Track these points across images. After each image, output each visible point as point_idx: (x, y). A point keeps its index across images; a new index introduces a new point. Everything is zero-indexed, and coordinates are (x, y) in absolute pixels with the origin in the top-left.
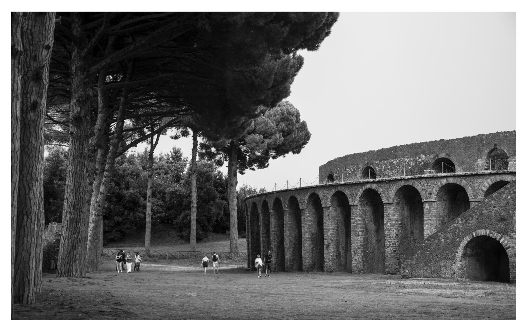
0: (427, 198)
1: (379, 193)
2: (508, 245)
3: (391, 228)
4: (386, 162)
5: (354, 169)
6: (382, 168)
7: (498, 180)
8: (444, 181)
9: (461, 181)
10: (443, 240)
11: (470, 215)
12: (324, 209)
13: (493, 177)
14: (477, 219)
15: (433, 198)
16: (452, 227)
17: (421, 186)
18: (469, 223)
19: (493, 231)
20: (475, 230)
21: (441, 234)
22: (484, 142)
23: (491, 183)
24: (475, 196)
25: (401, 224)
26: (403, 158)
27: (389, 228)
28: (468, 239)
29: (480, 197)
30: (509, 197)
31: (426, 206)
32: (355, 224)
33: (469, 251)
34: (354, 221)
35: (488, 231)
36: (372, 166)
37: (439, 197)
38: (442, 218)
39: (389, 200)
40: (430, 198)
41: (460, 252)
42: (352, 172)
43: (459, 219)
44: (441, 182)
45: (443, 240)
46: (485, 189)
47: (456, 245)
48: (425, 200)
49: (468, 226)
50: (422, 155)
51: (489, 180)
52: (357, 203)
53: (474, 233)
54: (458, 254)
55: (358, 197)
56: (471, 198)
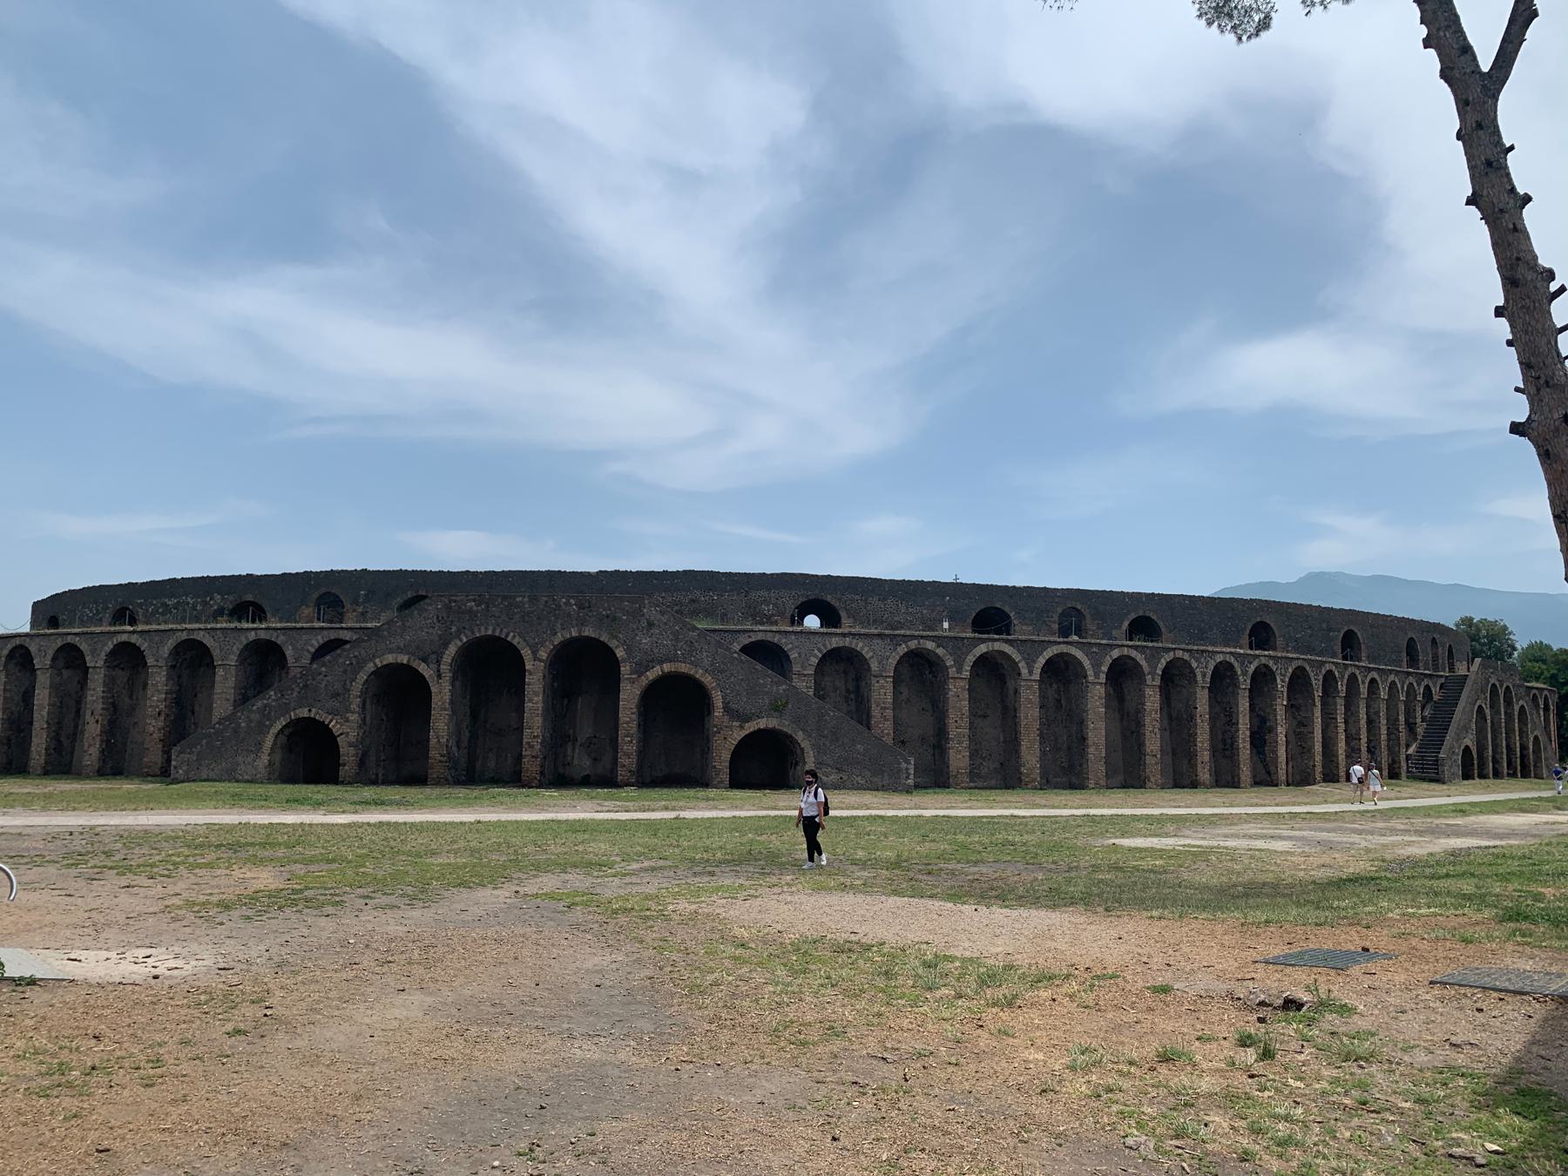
1: (142, 649)
2: (341, 731)
4: (154, 602)
5: (97, 610)
6: (147, 610)
7: (332, 638)
8: (252, 636)
9: (277, 637)
10: (243, 725)
12: (38, 672)
13: (325, 633)
14: (299, 692)
15: (233, 660)
16: (259, 704)
18: (287, 699)
19: (320, 711)
20: (295, 709)
21: (243, 714)
23: (321, 642)
24: (297, 660)
25: (175, 698)
26: (184, 598)
28: (283, 722)
29: (306, 661)
30: (348, 662)
31: (220, 672)
32: (94, 698)
33: (283, 739)
36: (131, 607)
37: (242, 659)
38: (243, 691)
39: (158, 661)
41: (269, 741)
42: (94, 614)
43: (272, 693)
44: (247, 638)
46: (313, 650)
47: (262, 729)
48: (220, 663)
49: (286, 703)
50: (215, 595)
51: (319, 637)
52: (100, 663)
53: (292, 713)
56: (290, 661)
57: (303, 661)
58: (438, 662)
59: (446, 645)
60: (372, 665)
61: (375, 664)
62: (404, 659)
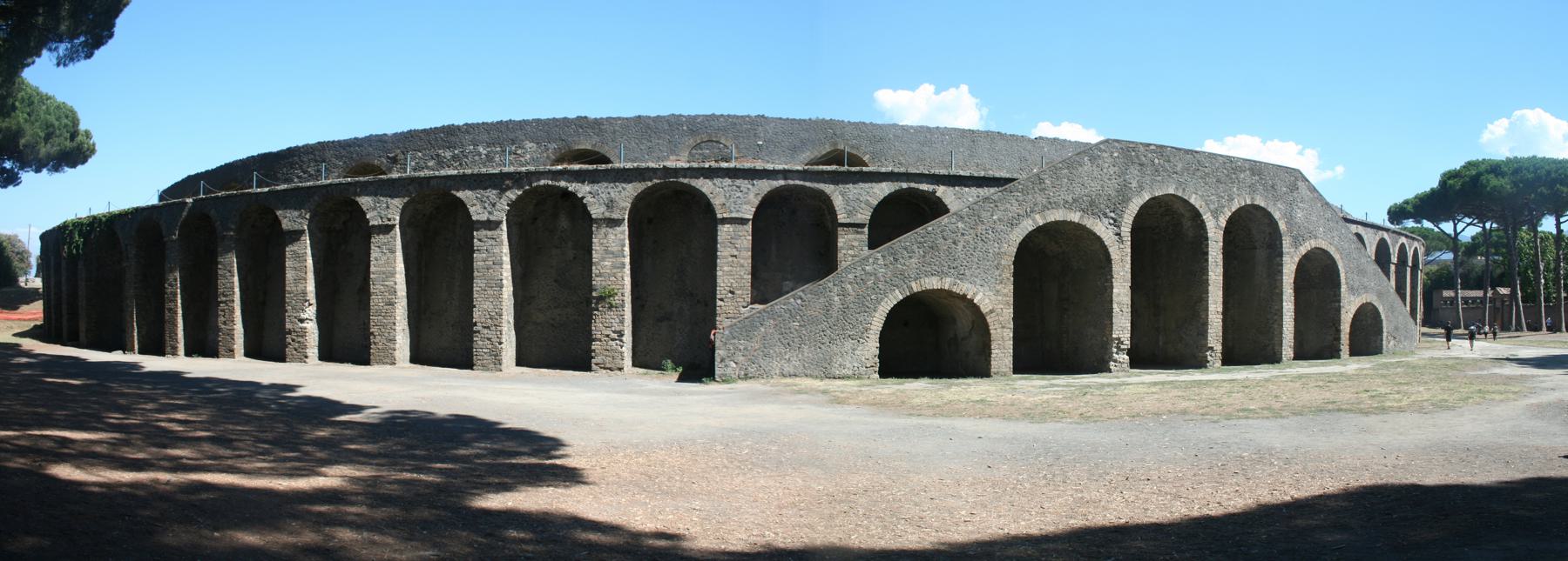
0: (731, 212)
3: (615, 271)
11: (906, 249)
17: (713, 186)
21: (834, 285)
22: (685, 128)
27: (608, 271)
34: (484, 255)
35: (948, 280)
40: (738, 211)
45: (836, 298)
47: (867, 309)
53: (913, 285)
54: (872, 327)
55: (505, 203)
57: (859, 216)
58: (1116, 223)
59: (1126, 200)
60: (1031, 222)
61: (1034, 220)
62: (1075, 217)
